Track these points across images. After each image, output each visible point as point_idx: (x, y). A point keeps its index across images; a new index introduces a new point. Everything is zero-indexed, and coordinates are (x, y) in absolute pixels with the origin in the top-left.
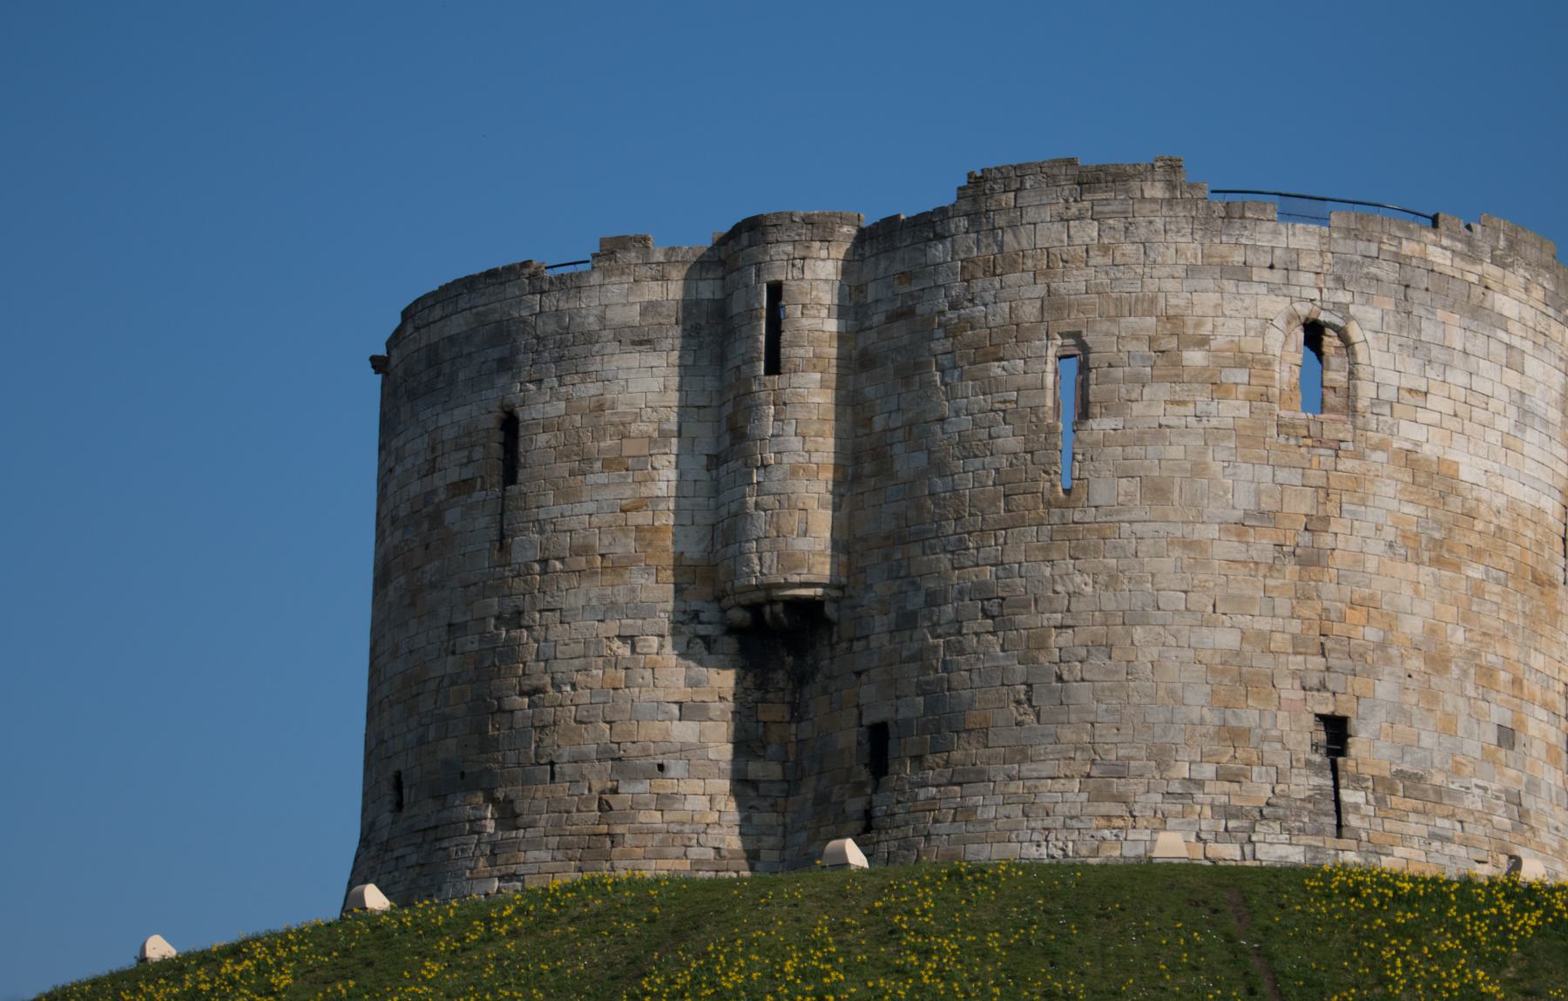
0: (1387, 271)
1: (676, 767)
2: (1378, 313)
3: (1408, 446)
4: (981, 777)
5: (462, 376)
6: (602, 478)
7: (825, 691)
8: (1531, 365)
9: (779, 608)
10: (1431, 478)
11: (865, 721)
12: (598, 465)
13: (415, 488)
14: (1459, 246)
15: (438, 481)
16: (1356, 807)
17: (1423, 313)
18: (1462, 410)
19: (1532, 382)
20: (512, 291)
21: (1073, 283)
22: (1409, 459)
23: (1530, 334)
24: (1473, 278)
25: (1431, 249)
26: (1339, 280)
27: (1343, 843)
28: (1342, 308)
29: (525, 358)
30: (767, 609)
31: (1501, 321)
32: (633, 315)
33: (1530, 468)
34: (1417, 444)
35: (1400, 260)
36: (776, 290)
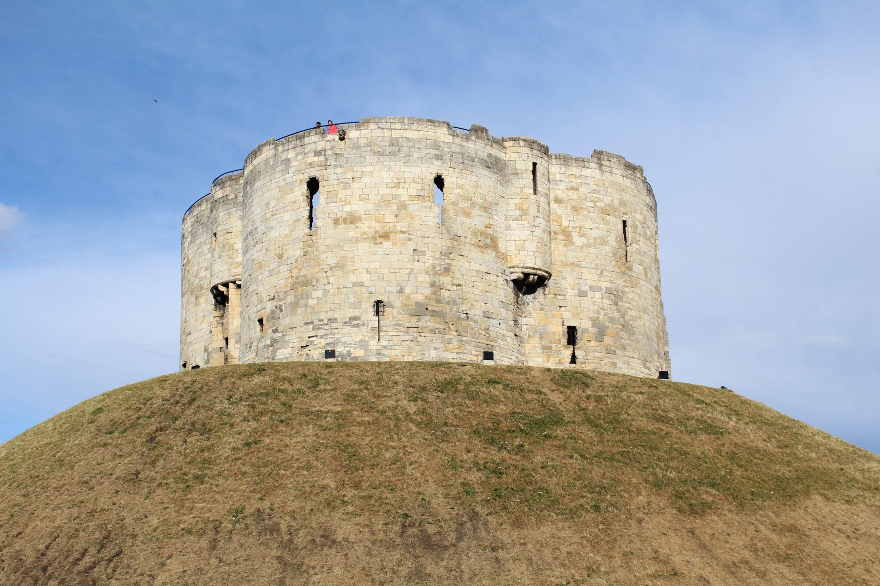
1: (503, 326)
4: (614, 353)
5: (415, 155)
6: (480, 213)
7: (541, 309)
9: (536, 277)
11: (567, 324)
12: (477, 207)
13: (383, 190)
15: (400, 191)
20: (439, 130)
21: (626, 197)
29: (447, 158)
30: (531, 277)
32: (484, 156)
36: (535, 164)
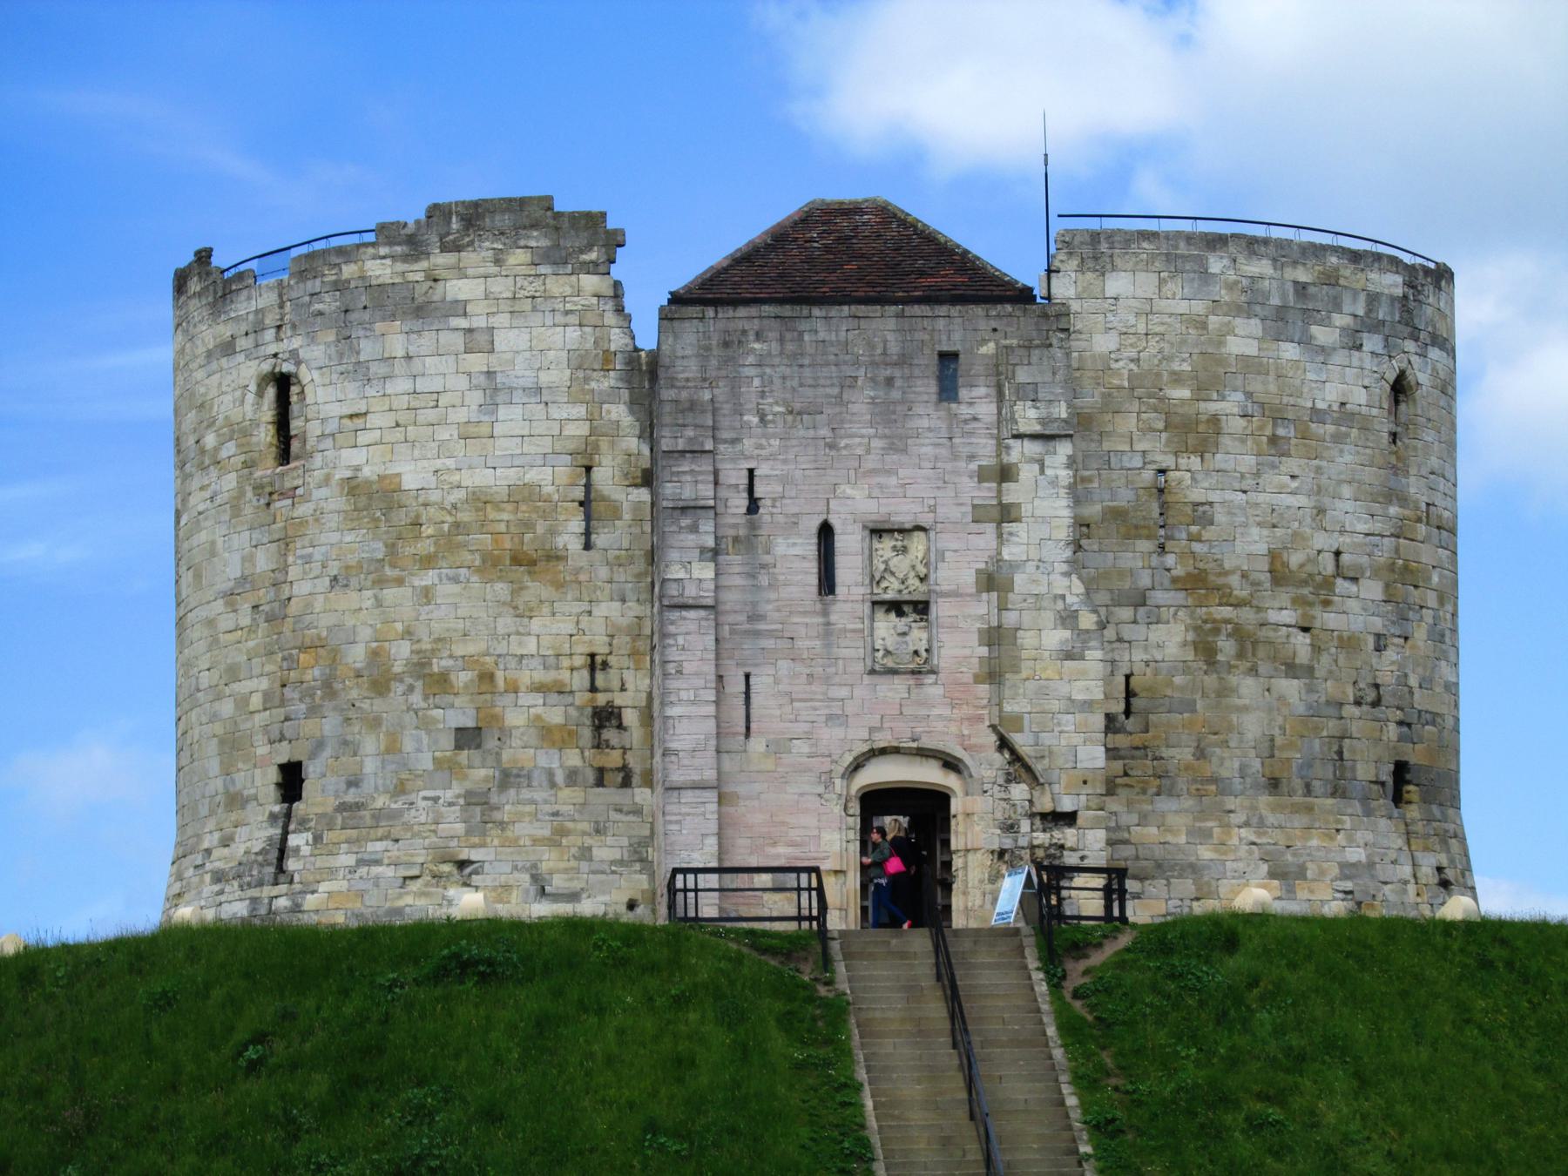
0: (329, 304)
2: (322, 347)
3: (349, 474)
8: (509, 339)
10: (373, 499)
14: (398, 249)
16: (297, 849)
17: (361, 333)
18: (403, 417)
19: (509, 356)
22: (353, 487)
23: (504, 306)
24: (420, 277)
25: (369, 264)
26: (294, 327)
27: (276, 890)
28: (294, 354)
31: (460, 308)
33: (504, 446)
34: (357, 469)
35: (340, 286)
